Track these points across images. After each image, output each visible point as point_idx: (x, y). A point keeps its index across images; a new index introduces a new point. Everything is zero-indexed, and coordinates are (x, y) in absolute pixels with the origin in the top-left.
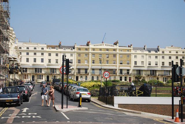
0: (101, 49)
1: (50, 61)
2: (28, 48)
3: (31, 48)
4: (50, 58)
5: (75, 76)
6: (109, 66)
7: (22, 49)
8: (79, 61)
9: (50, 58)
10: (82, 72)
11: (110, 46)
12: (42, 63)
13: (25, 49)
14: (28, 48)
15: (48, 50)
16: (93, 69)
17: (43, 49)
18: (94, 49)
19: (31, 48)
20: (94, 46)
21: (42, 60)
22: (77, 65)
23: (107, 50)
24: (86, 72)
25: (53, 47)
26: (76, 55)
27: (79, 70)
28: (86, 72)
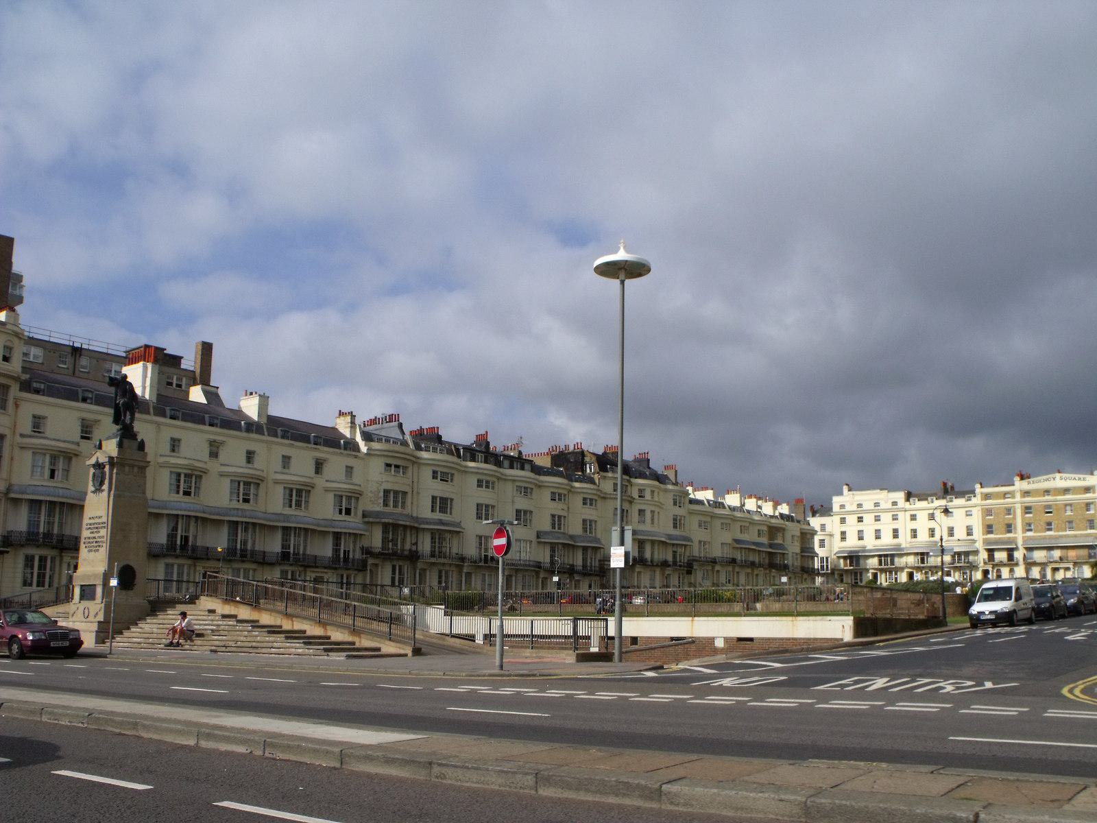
0: (1047, 492)
1: (914, 533)
2: (860, 505)
3: (868, 505)
4: (913, 525)
5: (981, 569)
6: (1075, 536)
7: (848, 508)
8: (989, 529)
9: (860, 527)
10: (1001, 556)
11: (1075, 479)
12: (896, 541)
13: (854, 508)
14: (860, 505)
15: (907, 505)
16: (1030, 549)
17: (895, 503)
18: (1026, 493)
19: (868, 505)
20: (1029, 483)
21: (896, 533)
22: (986, 542)
23: (1066, 491)
24: (1011, 557)
25: (922, 498)
26: (980, 513)
27: (991, 552)
28: (1011, 557)
